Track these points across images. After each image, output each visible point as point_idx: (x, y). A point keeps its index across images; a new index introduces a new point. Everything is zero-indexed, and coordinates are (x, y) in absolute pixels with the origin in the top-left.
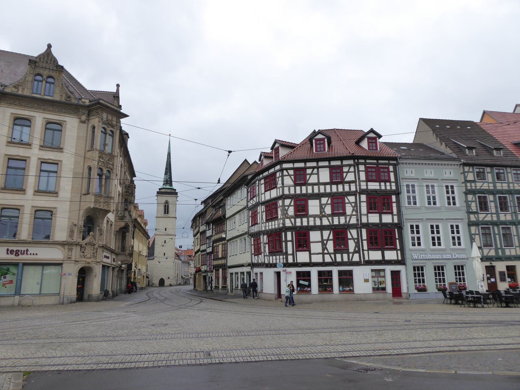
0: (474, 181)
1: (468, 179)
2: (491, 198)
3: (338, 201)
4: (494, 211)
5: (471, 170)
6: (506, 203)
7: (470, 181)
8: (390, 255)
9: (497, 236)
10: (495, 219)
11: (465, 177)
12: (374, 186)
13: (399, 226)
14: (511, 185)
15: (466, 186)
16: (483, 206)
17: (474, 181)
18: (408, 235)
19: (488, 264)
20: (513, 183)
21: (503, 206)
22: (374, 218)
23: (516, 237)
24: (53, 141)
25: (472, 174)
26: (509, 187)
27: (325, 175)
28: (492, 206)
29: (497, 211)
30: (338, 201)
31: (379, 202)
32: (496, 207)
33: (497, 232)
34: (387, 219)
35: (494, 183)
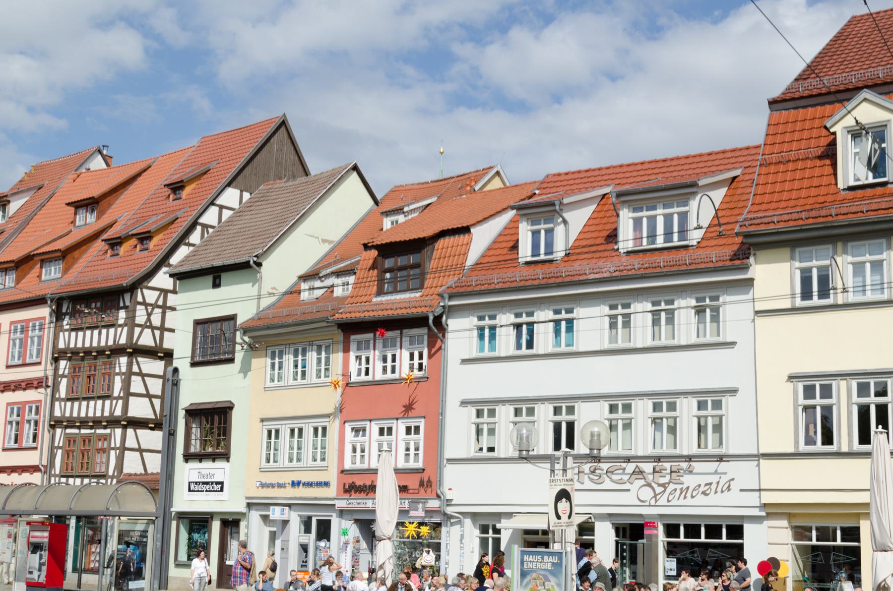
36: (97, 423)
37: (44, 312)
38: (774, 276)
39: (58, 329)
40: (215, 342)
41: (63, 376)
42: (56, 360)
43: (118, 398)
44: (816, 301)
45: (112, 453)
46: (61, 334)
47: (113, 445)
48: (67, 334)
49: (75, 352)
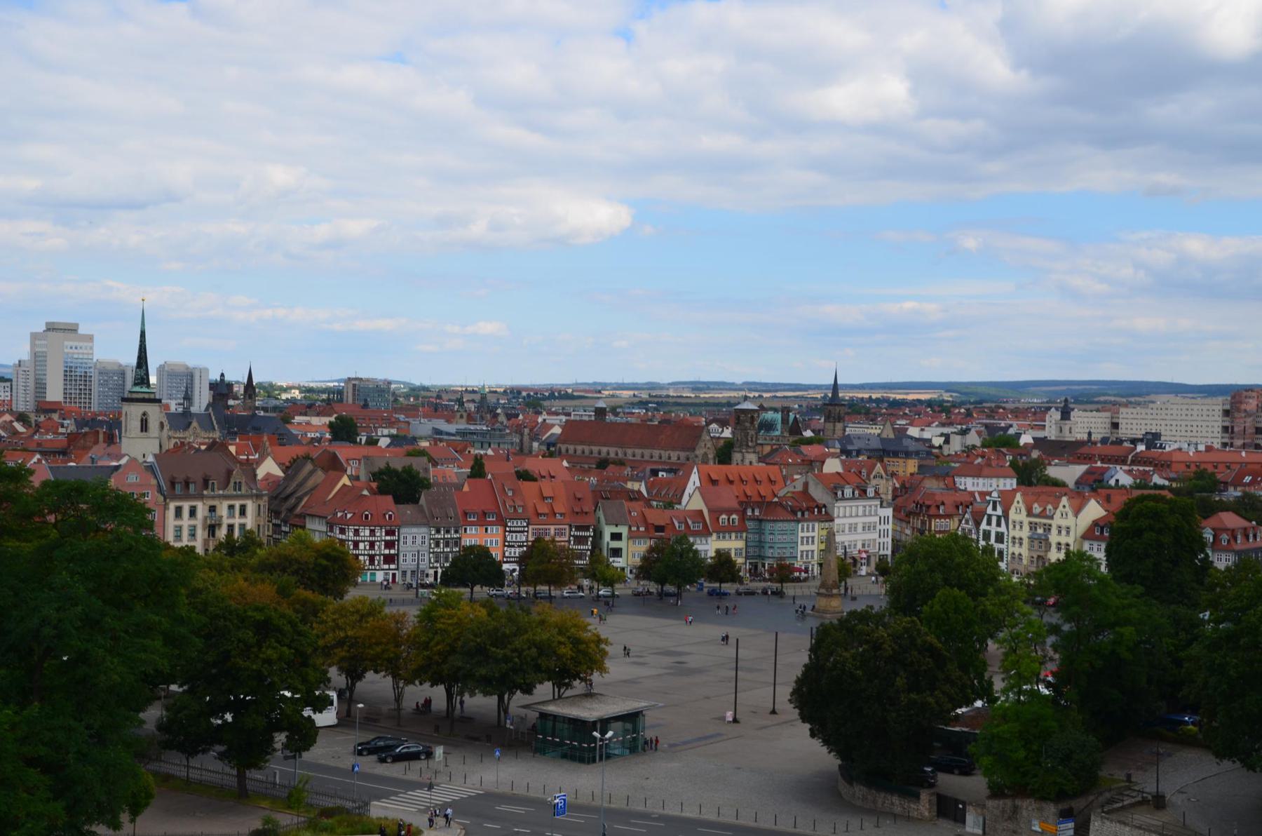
3: (372, 545)
8: (392, 566)
12: (388, 538)
13: (398, 555)
16: (437, 545)
18: (401, 558)
21: (447, 545)
22: (387, 552)
24: (243, 512)
27: (367, 533)
30: (372, 545)
31: (389, 545)
34: (392, 552)
38: (715, 535)
40: (617, 537)
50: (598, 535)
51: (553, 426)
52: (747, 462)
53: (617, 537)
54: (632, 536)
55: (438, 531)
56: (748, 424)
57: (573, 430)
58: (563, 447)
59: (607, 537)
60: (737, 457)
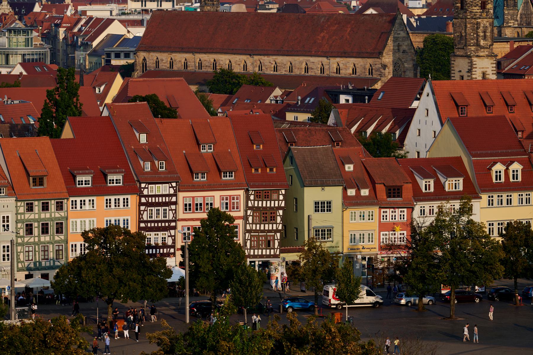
0: (24, 214)
1: (19, 212)
2: (36, 224)
4: (36, 235)
5: (22, 205)
6: (47, 229)
7: (21, 214)
9: (37, 253)
10: (37, 239)
11: (17, 211)
14: (53, 214)
15: (17, 217)
16: (29, 230)
17: (24, 214)
19: (27, 273)
20: (54, 212)
21: (45, 230)
23: (51, 253)
25: (23, 208)
26: (51, 215)
28: (36, 231)
29: (39, 234)
32: (39, 232)
33: (37, 250)
35: (39, 214)
36: (269, 231)
37: (241, 193)
39: (248, 199)
40: (323, 207)
41: (250, 215)
42: (246, 211)
43: (279, 224)
44: (491, 206)
45: (276, 241)
46: (249, 202)
47: (276, 238)
48: (253, 202)
49: (258, 207)
50: (294, 204)
51: (109, 22)
52: (477, 75)
53: (323, 207)
54: (348, 202)
55: (30, 208)
56: (477, 10)
57: (165, 30)
58: (152, 57)
59: (308, 208)
60: (459, 65)
